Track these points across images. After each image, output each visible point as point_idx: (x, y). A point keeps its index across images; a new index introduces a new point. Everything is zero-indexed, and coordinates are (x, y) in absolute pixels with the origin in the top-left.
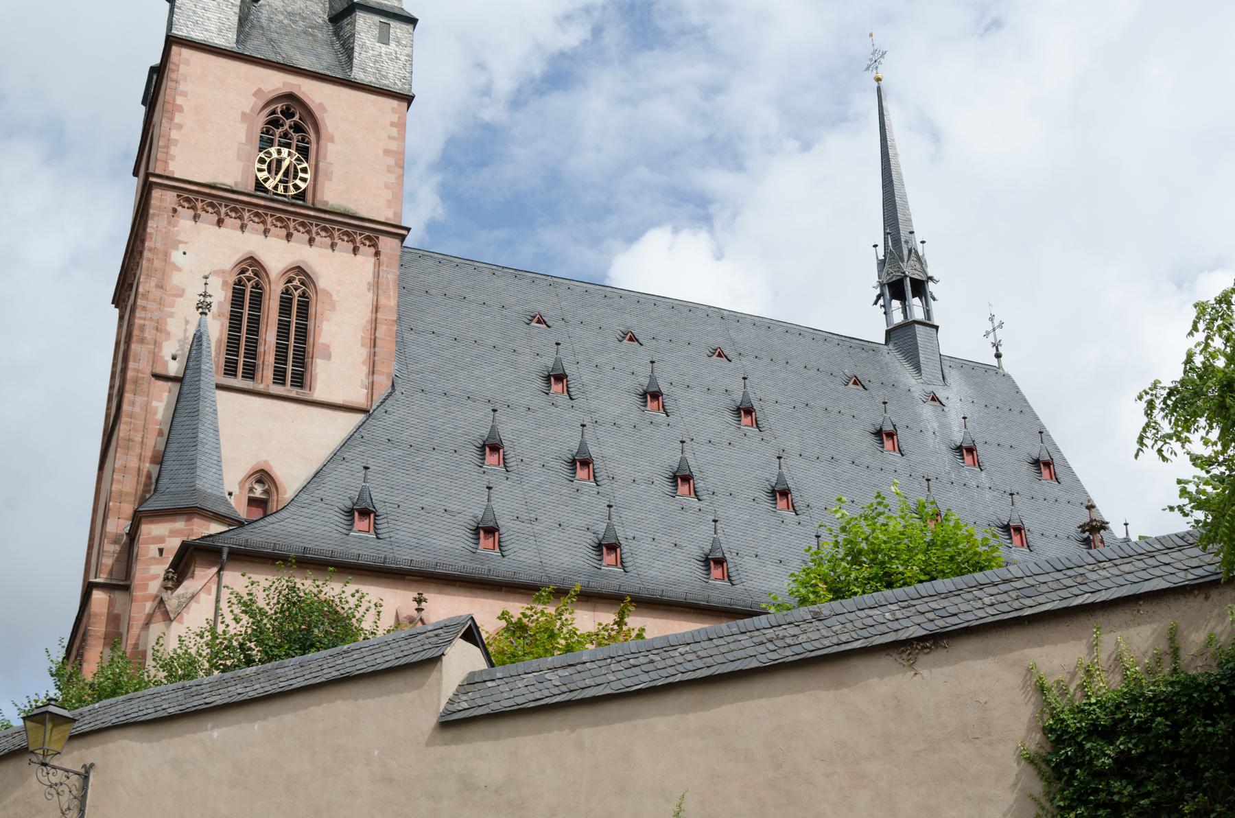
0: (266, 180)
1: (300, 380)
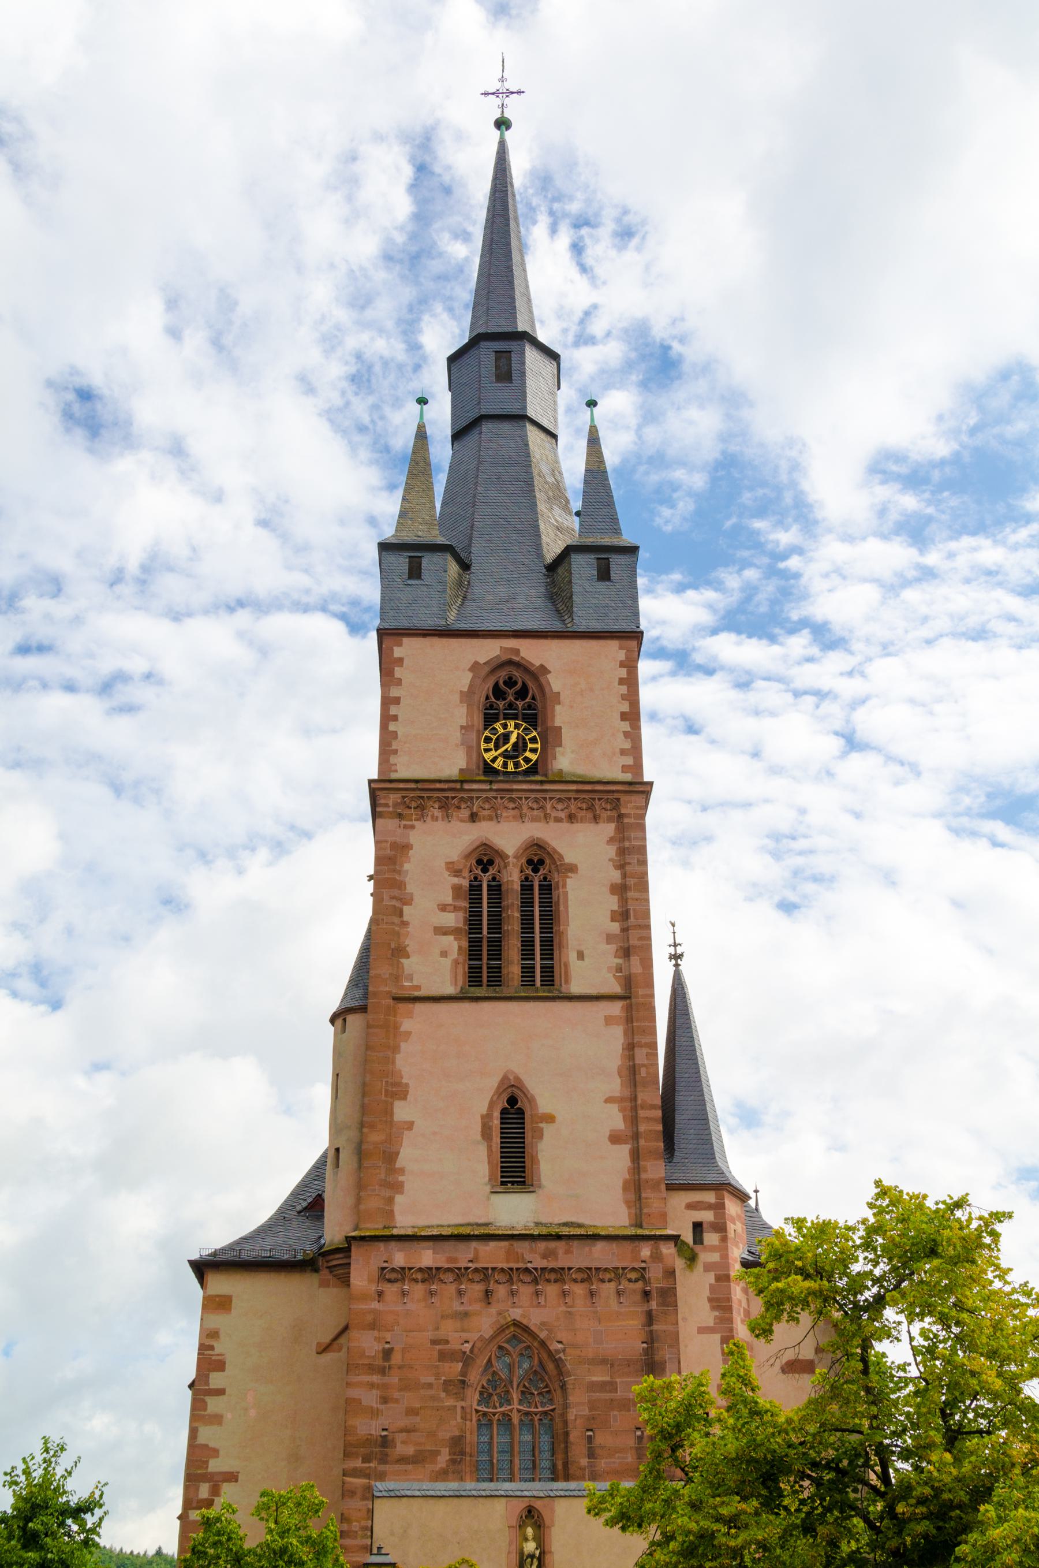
0: (494, 760)
1: (549, 975)
